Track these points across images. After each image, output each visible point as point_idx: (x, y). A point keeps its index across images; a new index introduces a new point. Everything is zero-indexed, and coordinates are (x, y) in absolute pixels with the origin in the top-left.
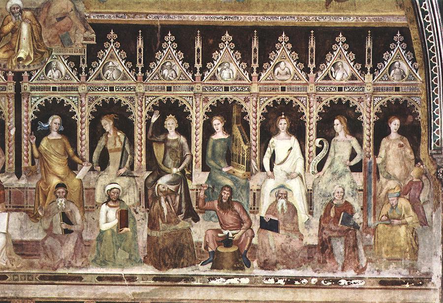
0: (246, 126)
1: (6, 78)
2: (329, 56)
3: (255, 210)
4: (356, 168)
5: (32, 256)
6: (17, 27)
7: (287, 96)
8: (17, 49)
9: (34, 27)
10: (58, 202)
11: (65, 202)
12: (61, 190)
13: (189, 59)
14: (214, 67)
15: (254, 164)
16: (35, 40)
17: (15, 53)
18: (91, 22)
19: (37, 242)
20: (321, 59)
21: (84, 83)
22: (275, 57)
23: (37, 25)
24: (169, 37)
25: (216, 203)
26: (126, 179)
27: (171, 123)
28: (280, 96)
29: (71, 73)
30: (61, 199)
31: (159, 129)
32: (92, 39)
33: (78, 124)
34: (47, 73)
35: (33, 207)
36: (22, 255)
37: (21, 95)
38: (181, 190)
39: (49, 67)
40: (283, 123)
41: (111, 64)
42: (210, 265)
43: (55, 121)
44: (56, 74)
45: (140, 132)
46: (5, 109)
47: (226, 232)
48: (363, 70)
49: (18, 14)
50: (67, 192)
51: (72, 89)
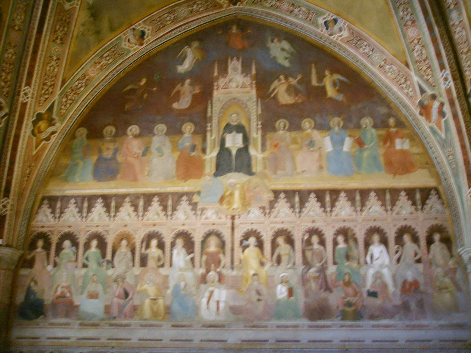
0: (356, 240)
2: (397, 203)
3: (364, 287)
4: (419, 261)
7: (378, 224)
12: (255, 277)
13: (323, 206)
14: (336, 210)
15: (362, 260)
20: (393, 204)
22: (368, 204)
24: (312, 195)
25: (341, 283)
26: (291, 271)
27: (315, 239)
28: (372, 224)
31: (308, 243)
38: (322, 276)
40: (376, 238)
41: (282, 210)
42: (340, 318)
43: (252, 240)
45: (298, 245)
47: (348, 299)
48: (416, 209)
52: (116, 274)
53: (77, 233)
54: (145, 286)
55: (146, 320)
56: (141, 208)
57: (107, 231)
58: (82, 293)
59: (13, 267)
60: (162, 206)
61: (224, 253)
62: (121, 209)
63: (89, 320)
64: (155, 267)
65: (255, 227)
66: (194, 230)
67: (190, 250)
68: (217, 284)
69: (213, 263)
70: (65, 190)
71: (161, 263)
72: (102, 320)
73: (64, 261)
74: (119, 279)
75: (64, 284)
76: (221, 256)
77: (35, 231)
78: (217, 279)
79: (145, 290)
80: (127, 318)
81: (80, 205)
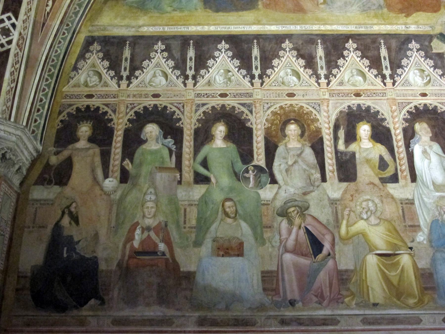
52: (283, 196)
53: (174, 109)
54: (361, 225)
55: (375, 305)
56: (321, 63)
57: (249, 106)
58: (198, 244)
59: (16, 181)
60: (367, 58)
62: (275, 62)
63: (227, 308)
64: (377, 181)
70: (140, 27)
71: (390, 172)
72: (262, 307)
73: (145, 170)
74: (292, 209)
75: (149, 222)
77: (70, 105)
79: (363, 234)
81: (177, 55)
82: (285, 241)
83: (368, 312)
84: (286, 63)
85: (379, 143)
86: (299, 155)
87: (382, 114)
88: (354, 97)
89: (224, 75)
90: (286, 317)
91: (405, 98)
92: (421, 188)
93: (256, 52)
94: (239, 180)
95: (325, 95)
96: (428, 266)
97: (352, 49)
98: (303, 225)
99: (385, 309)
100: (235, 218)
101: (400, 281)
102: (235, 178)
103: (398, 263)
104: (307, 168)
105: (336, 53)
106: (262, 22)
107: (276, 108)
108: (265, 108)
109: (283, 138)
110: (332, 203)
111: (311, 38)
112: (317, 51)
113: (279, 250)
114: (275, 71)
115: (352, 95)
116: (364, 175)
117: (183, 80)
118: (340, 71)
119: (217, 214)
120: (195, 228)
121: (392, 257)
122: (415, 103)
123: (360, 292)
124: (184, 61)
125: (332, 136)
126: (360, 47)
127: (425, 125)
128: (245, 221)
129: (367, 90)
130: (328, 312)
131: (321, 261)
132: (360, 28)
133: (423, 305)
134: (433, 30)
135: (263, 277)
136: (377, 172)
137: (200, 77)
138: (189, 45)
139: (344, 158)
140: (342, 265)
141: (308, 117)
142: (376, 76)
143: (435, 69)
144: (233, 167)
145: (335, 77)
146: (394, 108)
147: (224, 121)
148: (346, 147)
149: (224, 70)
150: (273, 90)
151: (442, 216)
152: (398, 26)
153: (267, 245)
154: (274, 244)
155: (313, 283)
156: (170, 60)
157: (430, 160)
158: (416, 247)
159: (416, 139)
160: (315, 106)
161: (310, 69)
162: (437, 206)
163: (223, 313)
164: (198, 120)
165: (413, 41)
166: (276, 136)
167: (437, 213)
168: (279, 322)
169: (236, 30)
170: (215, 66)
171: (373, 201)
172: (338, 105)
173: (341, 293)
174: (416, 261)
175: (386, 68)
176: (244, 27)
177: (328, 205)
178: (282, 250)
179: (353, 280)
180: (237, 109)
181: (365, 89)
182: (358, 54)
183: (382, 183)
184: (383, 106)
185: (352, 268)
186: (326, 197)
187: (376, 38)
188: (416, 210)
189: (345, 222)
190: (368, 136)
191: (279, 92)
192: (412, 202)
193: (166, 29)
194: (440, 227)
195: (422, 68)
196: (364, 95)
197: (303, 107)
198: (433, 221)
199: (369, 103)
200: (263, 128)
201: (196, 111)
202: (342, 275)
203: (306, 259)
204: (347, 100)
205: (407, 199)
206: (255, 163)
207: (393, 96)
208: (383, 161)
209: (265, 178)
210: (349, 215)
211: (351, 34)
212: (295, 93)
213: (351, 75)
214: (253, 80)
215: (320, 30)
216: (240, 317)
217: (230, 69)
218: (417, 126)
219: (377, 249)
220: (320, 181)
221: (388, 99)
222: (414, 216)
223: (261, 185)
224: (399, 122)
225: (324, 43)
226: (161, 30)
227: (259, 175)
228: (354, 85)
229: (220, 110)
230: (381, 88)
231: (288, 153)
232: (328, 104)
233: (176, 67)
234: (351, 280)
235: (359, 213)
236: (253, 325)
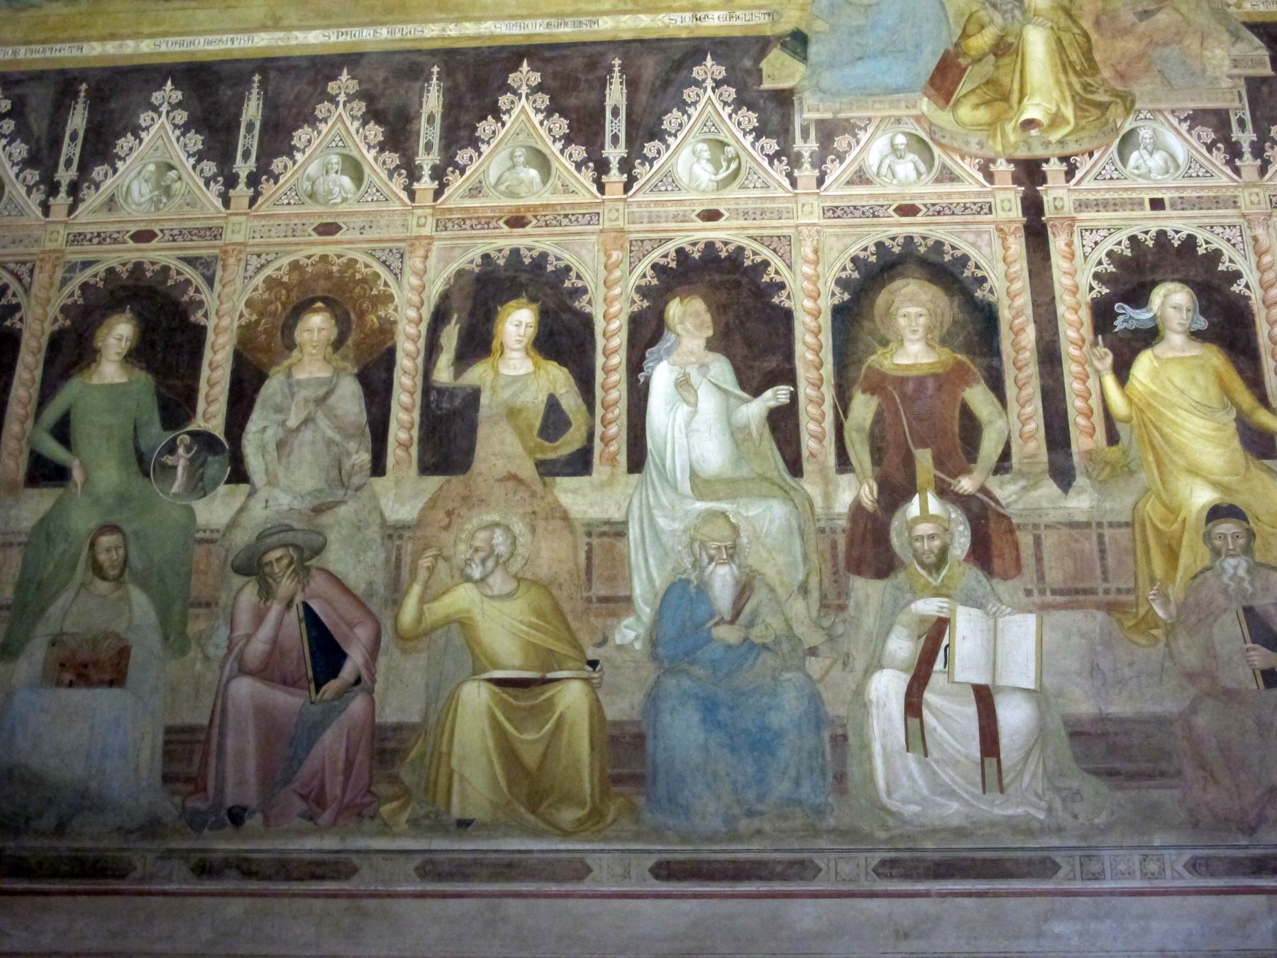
1: (990, 177)
5: (1150, 776)
6: (1011, 39)
8: (1015, 97)
9: (1066, 38)
10: (1223, 570)
11: (1249, 571)
12: (1227, 527)
16: (1074, 68)
17: (1011, 107)
18: (1247, 20)
19: (1162, 722)
21: (1254, 186)
23: (1076, 31)
29: (1205, 158)
30: (1232, 561)
32: (1261, 63)
33: (1255, 309)
34: (1123, 156)
35: (1128, 591)
36: (1111, 774)
37: (1044, 226)
39: (1128, 142)
44: (1157, 160)
46: (993, 268)
49: (1010, 6)
50: (1251, 535)
51: (1217, 202)
52: (259, 514)
54: (462, 598)
55: (464, 824)
56: (429, 132)
57: (206, 266)
60: (564, 114)
61: (996, 385)
62: (301, 136)
64: (528, 470)
65: (1178, 224)
66: (781, 243)
67: (771, 363)
68: (972, 576)
69: (924, 444)
71: (570, 442)
72: (152, 828)
76: (978, 397)
78: (961, 542)
79: (463, 624)
80: (327, 816)
81: (39, 125)
82: (241, 643)
83: (439, 844)
84: (330, 137)
85: (555, 360)
86: (321, 401)
87: (579, 277)
88: (506, 229)
89: (154, 178)
90: (214, 855)
91: (655, 226)
92: (654, 489)
93: (252, 110)
94: (147, 474)
95: (424, 225)
96: (636, 716)
97: (524, 90)
98: (298, 599)
99: (490, 837)
100: (118, 580)
101: (545, 756)
102: (135, 467)
103: (550, 703)
104: (338, 438)
105: (476, 102)
106: (286, 23)
107: (279, 269)
108: (251, 269)
109: (286, 352)
110: (390, 536)
111: (414, 63)
112: (424, 99)
113: (222, 668)
114: (295, 163)
115: (501, 223)
116: (494, 455)
117: (43, 197)
118: (480, 154)
119: (73, 568)
120: (8, 607)
121: (538, 689)
122: (681, 241)
123: (426, 789)
124: (56, 143)
125: (422, 343)
126: (550, 82)
127: (698, 305)
128: (145, 587)
129: (546, 206)
130: (330, 843)
131: (333, 700)
132: (559, 25)
133: (601, 826)
134: (774, 22)
135: (167, 743)
136: (532, 444)
137: (89, 187)
138: (75, 95)
139: (445, 405)
140: (387, 712)
141: (365, 290)
142: (578, 166)
143: (757, 138)
144: (136, 438)
145: (462, 172)
146: (616, 255)
147: (132, 310)
148: (458, 374)
149: (158, 165)
150: (279, 216)
151: (702, 570)
152: (673, 16)
153: (191, 654)
154: (211, 651)
155: (301, 763)
156: (18, 141)
157: (696, 405)
158: (608, 660)
159: (663, 345)
160: (391, 260)
161: (396, 152)
162: (693, 540)
163: (45, 843)
164: (64, 309)
165: (709, 57)
166: (268, 349)
167: (687, 562)
168: (192, 870)
169: (210, 48)
170: (134, 155)
171: (507, 529)
172: (457, 252)
173: (373, 789)
174: (601, 697)
175: (615, 139)
176: (232, 40)
177: (379, 540)
178: (231, 671)
179: (413, 754)
180: (173, 273)
181: (541, 205)
182: (539, 101)
183: (541, 475)
184: (584, 252)
185: (415, 718)
186: (375, 517)
187: (602, 54)
188: (629, 552)
189: (416, 589)
190: (526, 341)
191: (296, 221)
192: (620, 528)
193: (23, 53)
194: (691, 599)
195: (721, 137)
196: (534, 222)
197: (356, 261)
198: (673, 584)
199: (545, 244)
200: (236, 324)
201: (64, 282)
202: (384, 740)
203: (291, 694)
204: (484, 237)
205: (608, 522)
206: (198, 424)
207: (620, 224)
208: (555, 412)
209: (216, 466)
210: (431, 570)
211: (530, 46)
212: (340, 221)
213: (509, 164)
214: (51, 199)
215: (444, 38)
216: (91, 855)
217: (175, 162)
218: (673, 309)
219: (496, 666)
220: (368, 472)
221: (601, 231)
222: (619, 568)
223: (203, 488)
224: (624, 297)
225: (447, 74)
226: (9, 56)
227: (201, 459)
228: (513, 195)
229: (128, 278)
230: (588, 199)
231: (293, 395)
232: (428, 251)
233: (30, 162)
234: (406, 752)
235: (462, 564)
236: (122, 876)
